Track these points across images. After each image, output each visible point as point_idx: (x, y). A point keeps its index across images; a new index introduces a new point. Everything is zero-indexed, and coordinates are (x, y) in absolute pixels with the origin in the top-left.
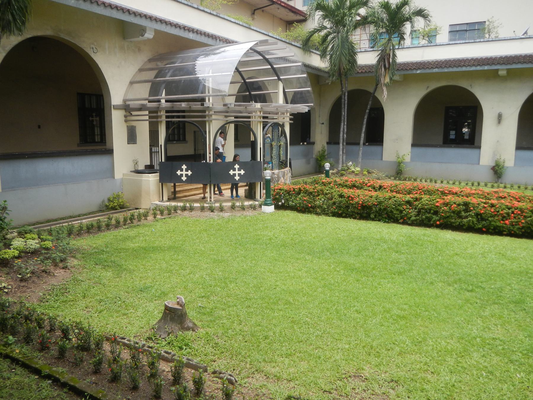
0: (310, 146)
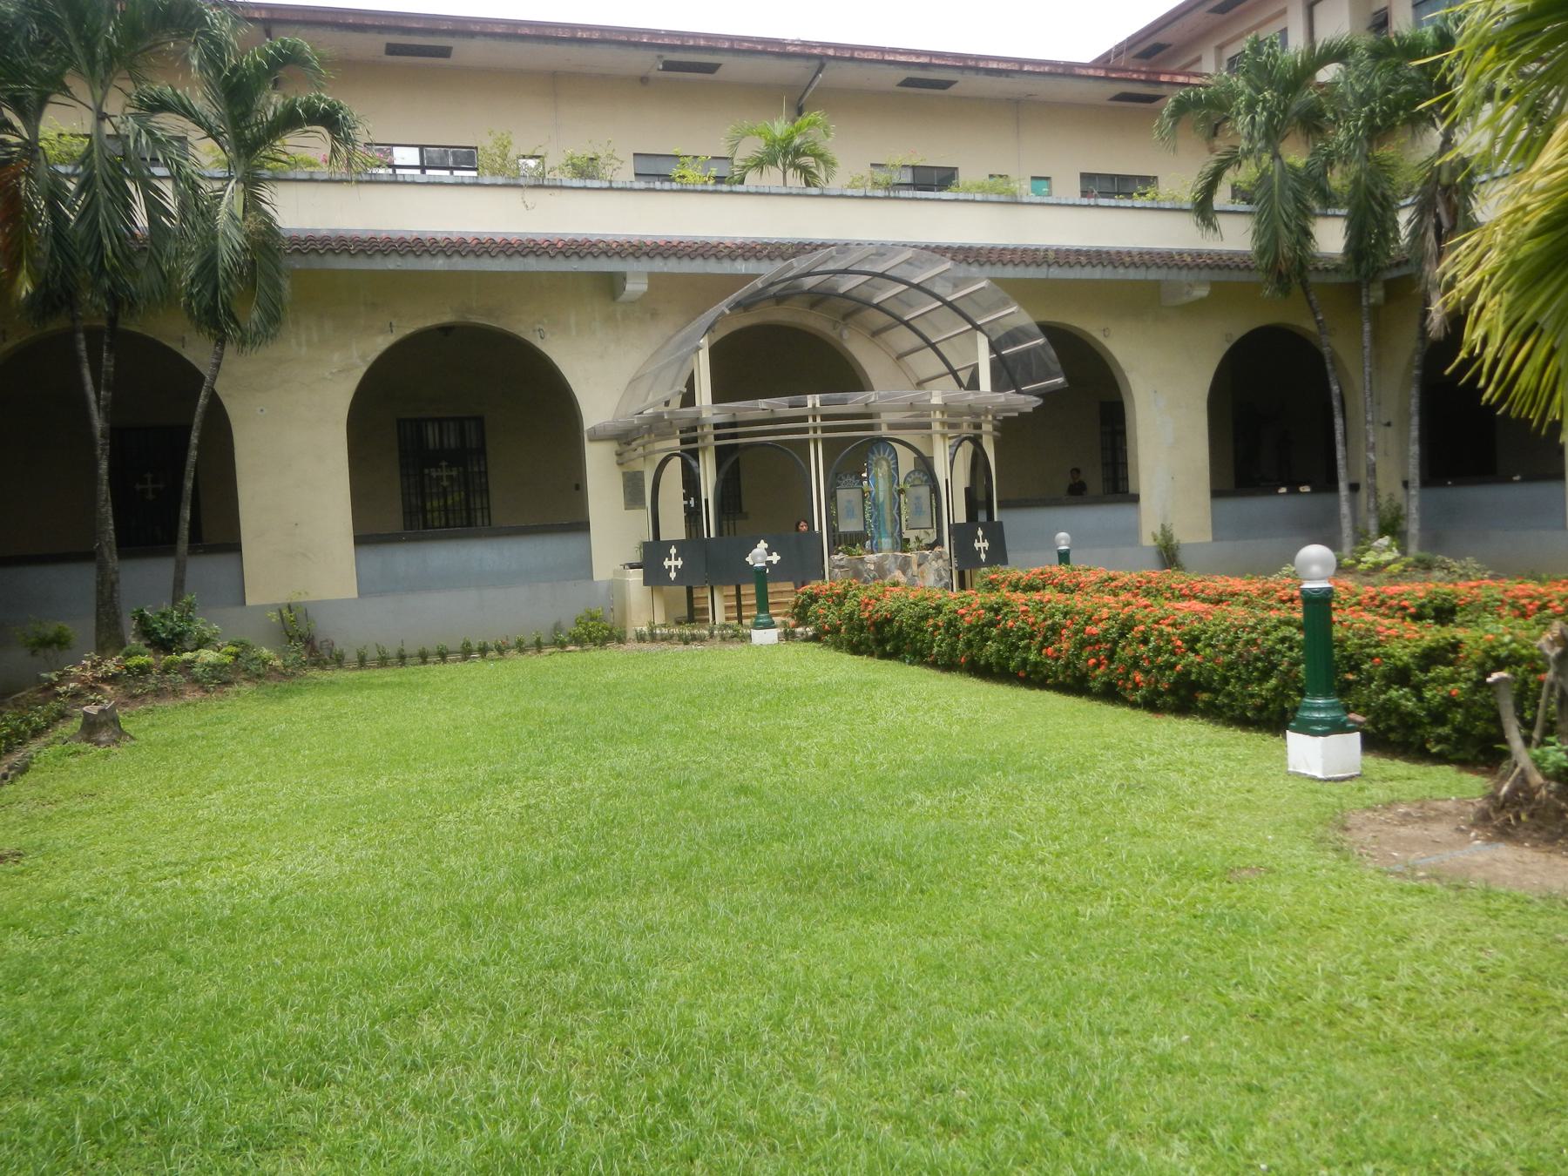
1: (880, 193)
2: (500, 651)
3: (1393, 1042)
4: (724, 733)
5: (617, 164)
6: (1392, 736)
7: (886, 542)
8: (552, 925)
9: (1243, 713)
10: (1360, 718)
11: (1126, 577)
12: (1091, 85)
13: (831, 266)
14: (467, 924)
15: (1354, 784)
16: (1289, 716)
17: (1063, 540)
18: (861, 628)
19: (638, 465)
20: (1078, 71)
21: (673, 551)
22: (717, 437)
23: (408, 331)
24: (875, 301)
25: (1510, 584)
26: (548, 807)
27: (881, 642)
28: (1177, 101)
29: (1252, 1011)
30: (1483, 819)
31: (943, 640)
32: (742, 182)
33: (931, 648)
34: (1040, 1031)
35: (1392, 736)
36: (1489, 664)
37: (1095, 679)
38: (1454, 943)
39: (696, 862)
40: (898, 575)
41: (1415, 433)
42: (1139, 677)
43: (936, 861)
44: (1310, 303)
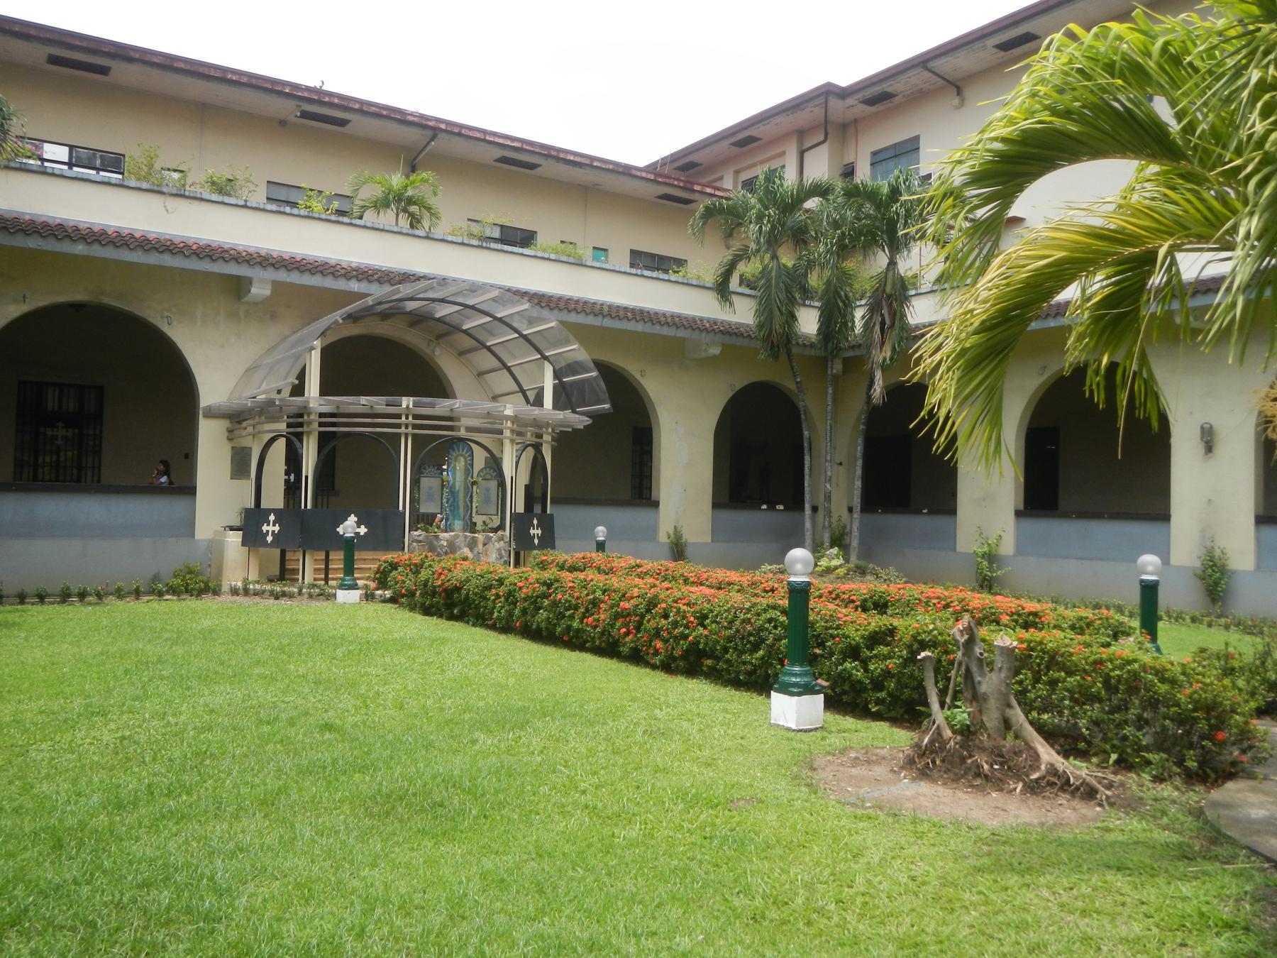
1: (475, 242)
2: (99, 596)
3: (855, 936)
4: (311, 677)
5: (253, 187)
6: (845, 698)
7: (458, 524)
8: (144, 847)
9: (737, 676)
10: (825, 684)
11: (649, 565)
12: (643, 183)
13: (431, 295)
14: (59, 846)
15: (818, 734)
16: (771, 680)
17: (601, 532)
18: (434, 594)
19: (246, 442)
20: (634, 172)
21: (272, 518)
22: (321, 425)
23: (42, 302)
24: (465, 327)
25: (923, 587)
26: (143, 738)
27: (450, 606)
28: (707, 208)
29: (750, 915)
30: (910, 762)
31: (502, 607)
32: (361, 218)
33: (492, 613)
34: (586, 935)
35: (845, 698)
36: (916, 646)
37: (625, 644)
38: (893, 858)
39: (284, 789)
40: (466, 551)
41: (859, 472)
42: (659, 644)
43: (497, 792)
44: (792, 368)
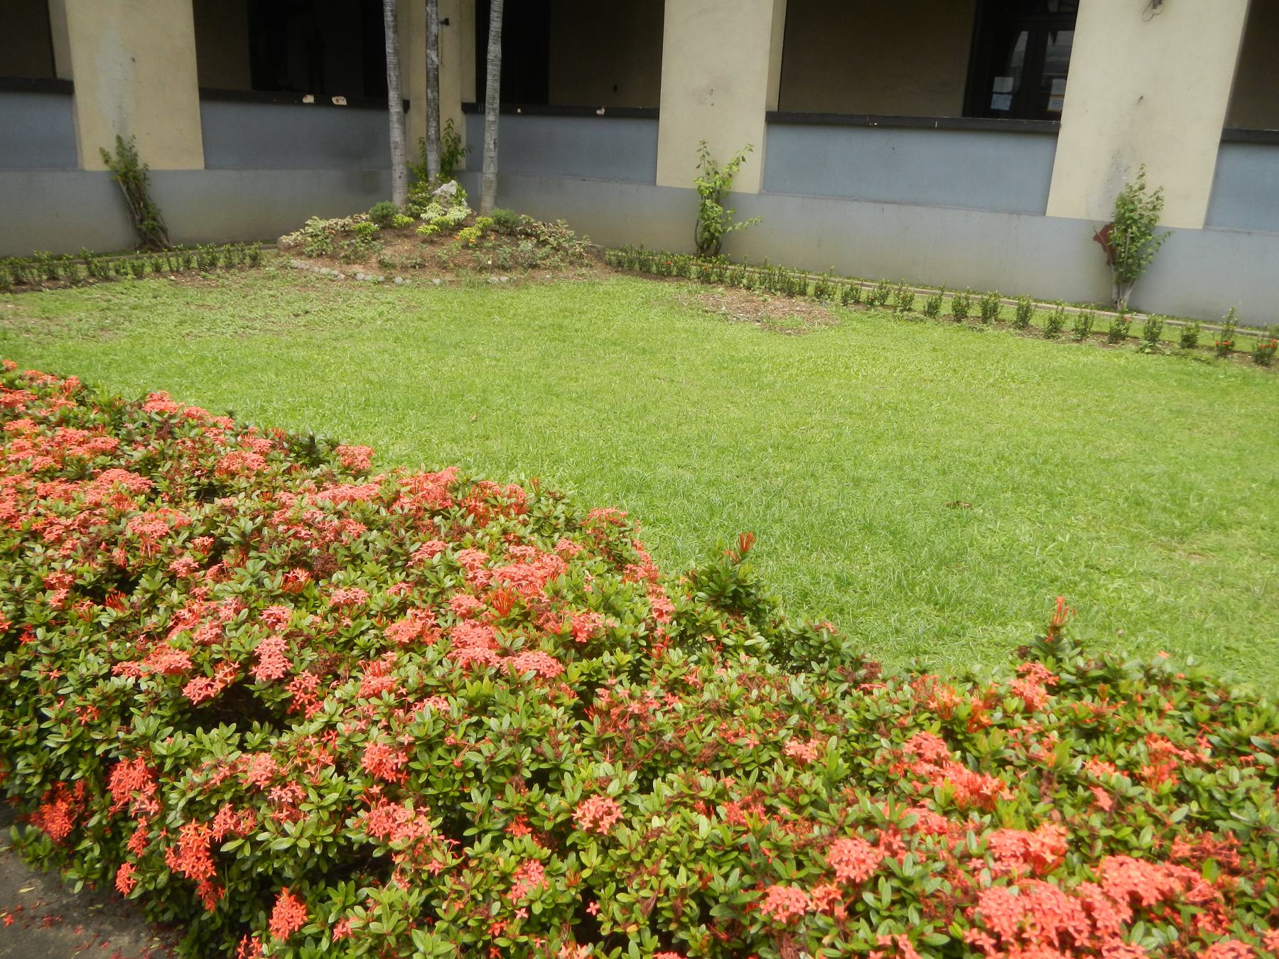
0: (364, 119)
41: (496, 25)
